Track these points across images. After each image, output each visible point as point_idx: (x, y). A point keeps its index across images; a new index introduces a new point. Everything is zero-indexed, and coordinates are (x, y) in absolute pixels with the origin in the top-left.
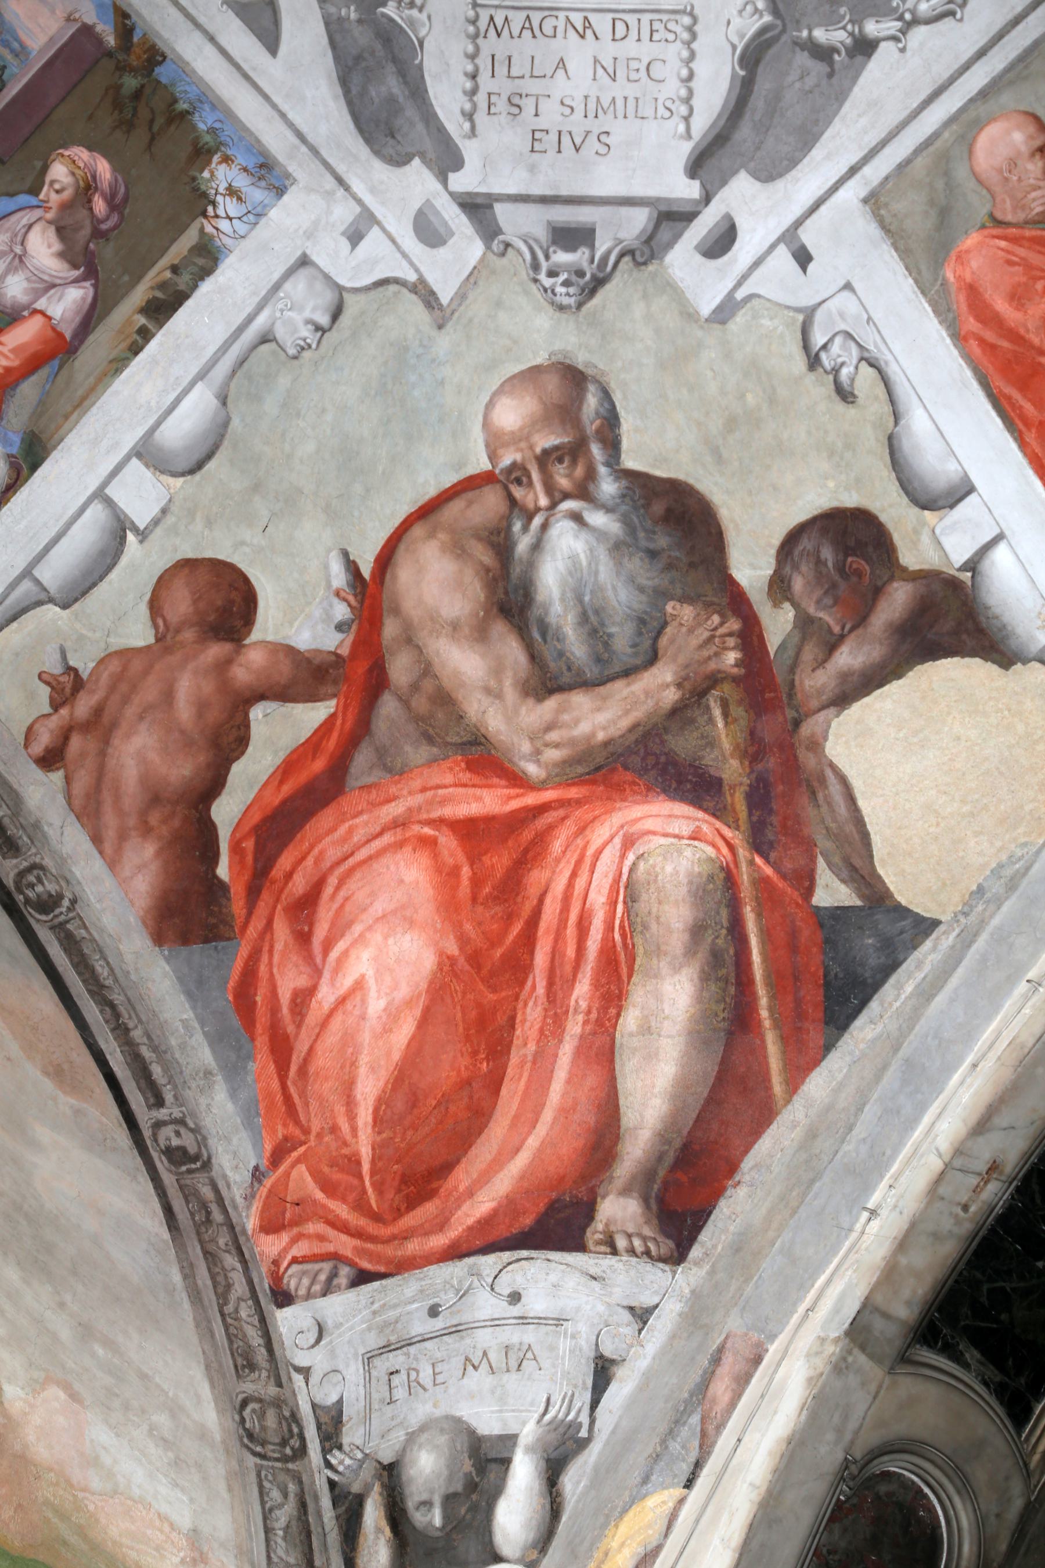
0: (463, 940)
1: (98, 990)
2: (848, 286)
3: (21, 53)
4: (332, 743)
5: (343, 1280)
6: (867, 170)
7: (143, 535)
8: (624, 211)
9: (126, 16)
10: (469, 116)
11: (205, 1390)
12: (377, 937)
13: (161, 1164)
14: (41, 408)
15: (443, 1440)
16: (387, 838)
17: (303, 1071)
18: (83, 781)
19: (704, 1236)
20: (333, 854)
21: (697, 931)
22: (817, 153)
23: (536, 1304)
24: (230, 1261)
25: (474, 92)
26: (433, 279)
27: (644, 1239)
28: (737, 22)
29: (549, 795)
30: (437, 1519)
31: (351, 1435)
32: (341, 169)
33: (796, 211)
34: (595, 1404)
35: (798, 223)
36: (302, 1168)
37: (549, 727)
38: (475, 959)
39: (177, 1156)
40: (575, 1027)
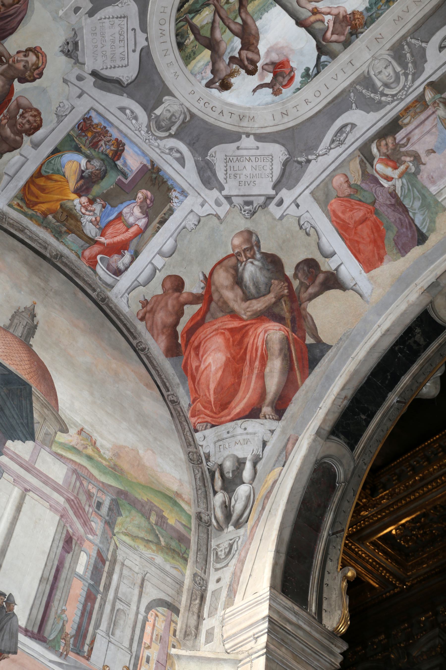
0: (231, 354)
1: (154, 367)
2: (307, 211)
3: (131, 171)
4: (202, 313)
5: (209, 427)
6: (310, 187)
7: (160, 271)
8: (259, 197)
9: (153, 162)
10: (226, 179)
11: (181, 450)
12: (213, 354)
13: (169, 404)
14: (138, 244)
15: (231, 459)
16: (214, 333)
17: (198, 383)
18: (149, 324)
19: (285, 414)
20: (203, 337)
21: (281, 350)
22: (300, 184)
23: (250, 430)
24: (185, 423)
25: (226, 174)
26: (219, 214)
27: (272, 416)
28: (281, 157)
29: (248, 322)
30: (231, 475)
31: (212, 459)
32: (199, 191)
33: (296, 196)
34: (263, 450)
35: (296, 198)
36: (199, 403)
37: (248, 308)
38: (234, 358)
39: (173, 402)
40: (256, 371)
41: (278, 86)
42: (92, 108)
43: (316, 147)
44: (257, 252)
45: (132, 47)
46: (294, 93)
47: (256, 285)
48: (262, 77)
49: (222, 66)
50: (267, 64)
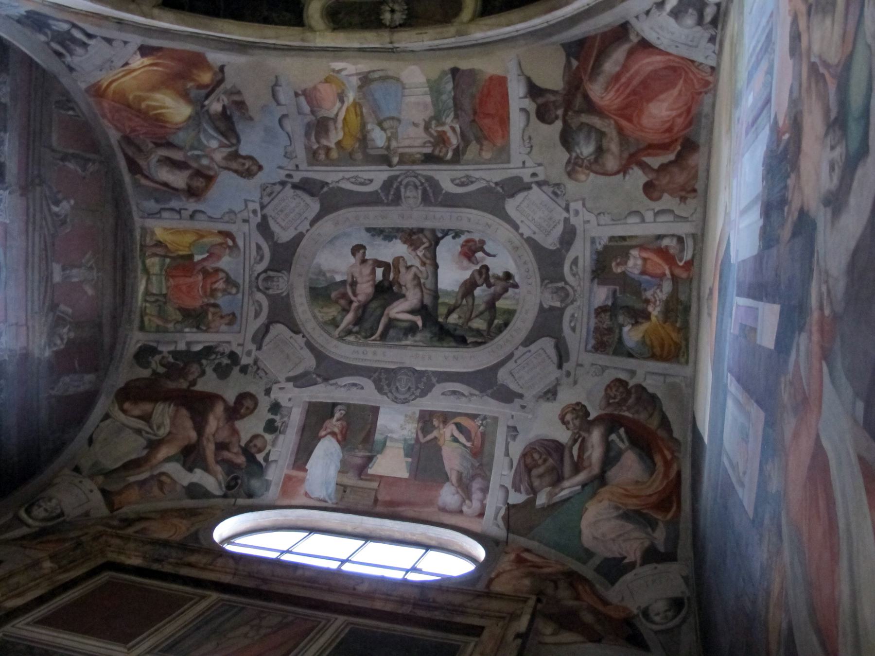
41: (478, 245)
42: (586, 351)
43: (485, 188)
44: (573, 157)
45: (528, 354)
46: (472, 232)
47: (588, 137)
48: (484, 259)
49: (498, 288)
50: (473, 263)
